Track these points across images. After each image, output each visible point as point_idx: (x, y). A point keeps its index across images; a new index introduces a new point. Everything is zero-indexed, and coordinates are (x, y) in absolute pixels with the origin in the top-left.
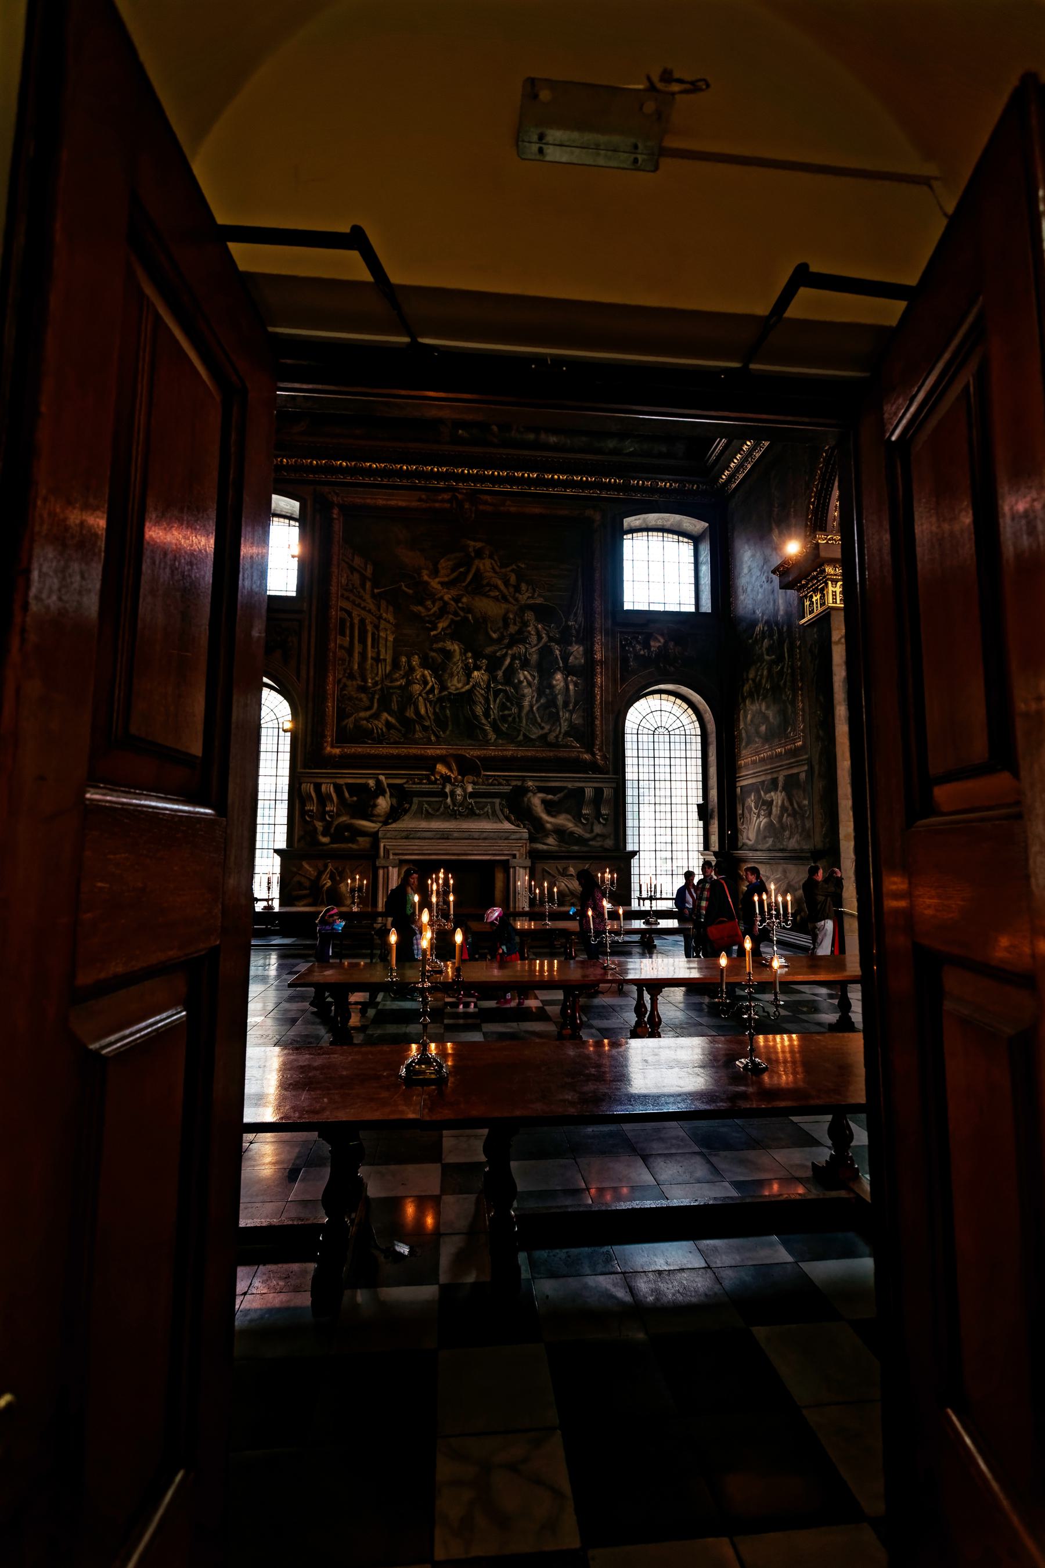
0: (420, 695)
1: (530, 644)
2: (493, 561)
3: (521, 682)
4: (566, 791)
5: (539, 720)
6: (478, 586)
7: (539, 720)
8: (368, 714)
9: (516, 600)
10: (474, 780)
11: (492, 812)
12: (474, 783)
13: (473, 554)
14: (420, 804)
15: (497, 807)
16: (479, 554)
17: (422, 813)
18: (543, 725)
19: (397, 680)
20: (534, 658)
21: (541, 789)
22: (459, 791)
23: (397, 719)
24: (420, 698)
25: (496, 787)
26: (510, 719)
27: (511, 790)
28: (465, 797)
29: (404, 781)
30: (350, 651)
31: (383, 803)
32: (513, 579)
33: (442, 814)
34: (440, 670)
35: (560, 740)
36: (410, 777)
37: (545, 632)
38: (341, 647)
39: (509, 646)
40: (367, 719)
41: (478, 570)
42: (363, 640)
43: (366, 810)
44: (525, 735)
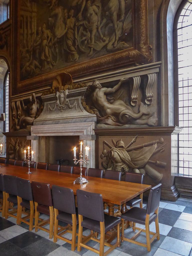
0: (46, 45)
3: (91, 14)
4: (120, 83)
5: (102, 36)
10: (69, 87)
11: (77, 106)
12: (69, 89)
15: (80, 102)
18: (105, 38)
19: (38, 41)
21: (104, 85)
22: (62, 95)
24: (47, 47)
26: (86, 42)
27: (87, 89)
28: (65, 98)
29: (41, 94)
31: (35, 107)
33: (55, 110)
34: (52, 28)
35: (115, 45)
40: (29, 66)
42: (27, 28)
43: (28, 112)
44: (94, 49)
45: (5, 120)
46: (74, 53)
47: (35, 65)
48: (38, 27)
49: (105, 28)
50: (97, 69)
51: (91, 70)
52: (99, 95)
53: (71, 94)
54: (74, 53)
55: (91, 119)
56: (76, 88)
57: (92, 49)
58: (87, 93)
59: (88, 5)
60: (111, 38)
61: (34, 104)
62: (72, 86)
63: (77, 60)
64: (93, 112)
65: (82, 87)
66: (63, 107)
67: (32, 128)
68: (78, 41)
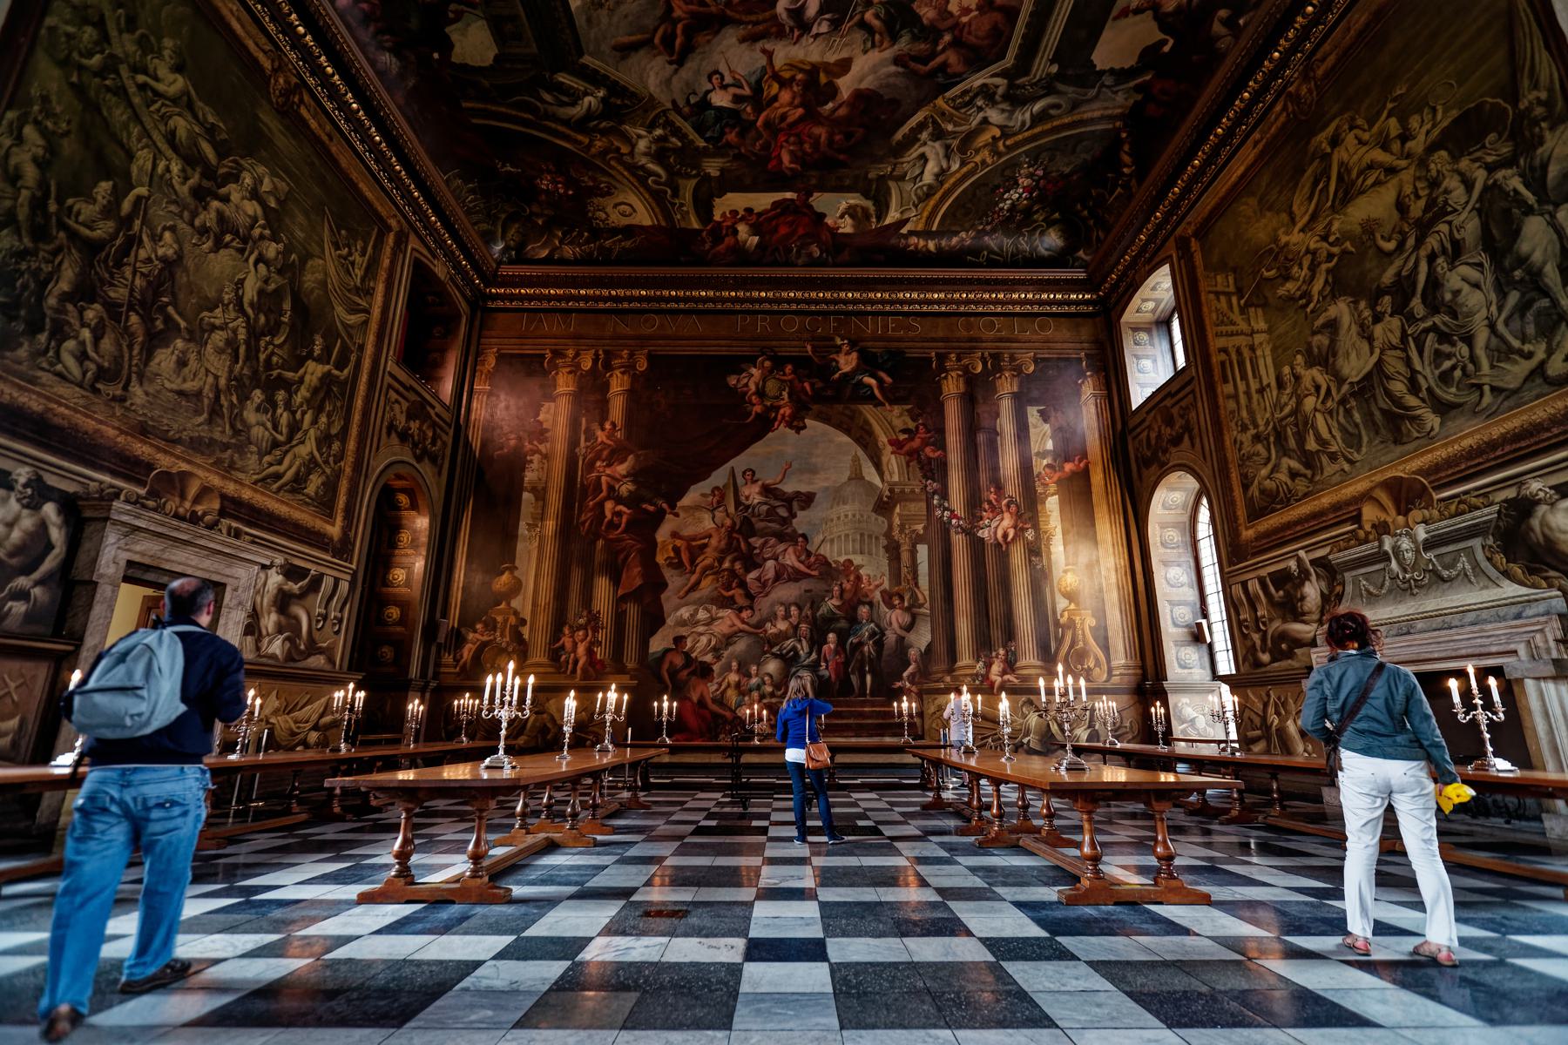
0: (1316, 410)
1: (1455, 210)
2: (1356, 131)
3: (1457, 293)
5: (1516, 344)
6: (1348, 192)
7: (1516, 344)
8: (1270, 466)
9: (1409, 156)
11: (1473, 569)
12: (1425, 522)
13: (1329, 150)
14: (1356, 582)
15: (1480, 556)
16: (1335, 141)
17: (1361, 595)
18: (1527, 348)
19: (1286, 404)
20: (1470, 228)
22: (1405, 544)
23: (1300, 462)
24: (1318, 415)
25: (1468, 516)
26: (1458, 373)
27: (1499, 512)
28: (1417, 552)
29: (1328, 549)
30: (1236, 397)
32: (1394, 126)
33: (1390, 591)
34: (1325, 360)
36: (1335, 543)
37: (1477, 164)
38: (1229, 397)
39: (1419, 242)
40: (1269, 477)
41: (1341, 164)
42: (1244, 377)
44: (1493, 389)
45: (1208, 640)
46: (1418, 412)
47: (1290, 469)
48: (1278, 366)
49: (1522, 316)
50: (1523, 444)
51: (1499, 453)
52: (1554, 525)
53: (1439, 535)
54: (1419, 412)
55: (1541, 607)
56: (1452, 517)
57: (1486, 388)
58: (1501, 524)
59: (1439, 269)
60: (1554, 344)
61: (1307, 583)
62: (1435, 513)
63: (1437, 429)
64: (1544, 584)
65: (1478, 508)
66: (1415, 580)
67: (1314, 657)
68: (1425, 378)
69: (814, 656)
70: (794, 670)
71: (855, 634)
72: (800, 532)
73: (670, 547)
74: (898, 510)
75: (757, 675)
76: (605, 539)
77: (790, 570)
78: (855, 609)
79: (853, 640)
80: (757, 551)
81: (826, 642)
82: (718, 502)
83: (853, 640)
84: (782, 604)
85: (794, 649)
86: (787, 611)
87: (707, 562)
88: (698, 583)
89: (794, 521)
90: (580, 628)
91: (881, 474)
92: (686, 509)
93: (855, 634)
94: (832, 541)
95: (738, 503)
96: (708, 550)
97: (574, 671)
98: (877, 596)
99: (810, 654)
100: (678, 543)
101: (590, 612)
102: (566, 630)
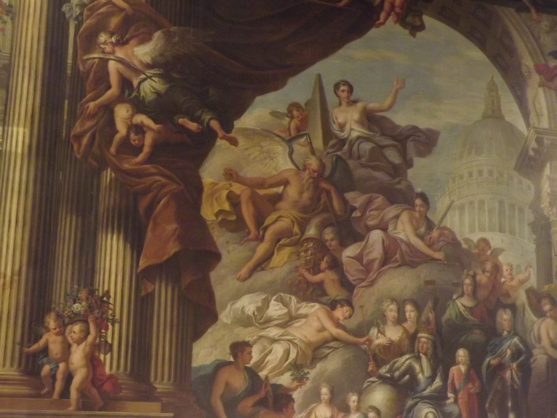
69: (438, 382)
70: (410, 402)
71: (493, 352)
72: (419, 190)
73: (225, 193)
74: (547, 171)
75: (358, 409)
76: (117, 169)
77: (403, 247)
78: (492, 314)
79: (491, 360)
80: (357, 214)
81: (453, 362)
82: (298, 129)
83: (491, 360)
84: (393, 300)
85: (410, 370)
86: (401, 312)
87: (283, 224)
88: (268, 257)
89: (410, 172)
90: (75, 318)
91: (526, 115)
92: (248, 133)
93: (493, 352)
94: (462, 208)
95: (328, 134)
96: (282, 205)
97: (65, 393)
98: (522, 298)
99: (432, 379)
100: (237, 188)
101: (92, 292)
102: (51, 322)
